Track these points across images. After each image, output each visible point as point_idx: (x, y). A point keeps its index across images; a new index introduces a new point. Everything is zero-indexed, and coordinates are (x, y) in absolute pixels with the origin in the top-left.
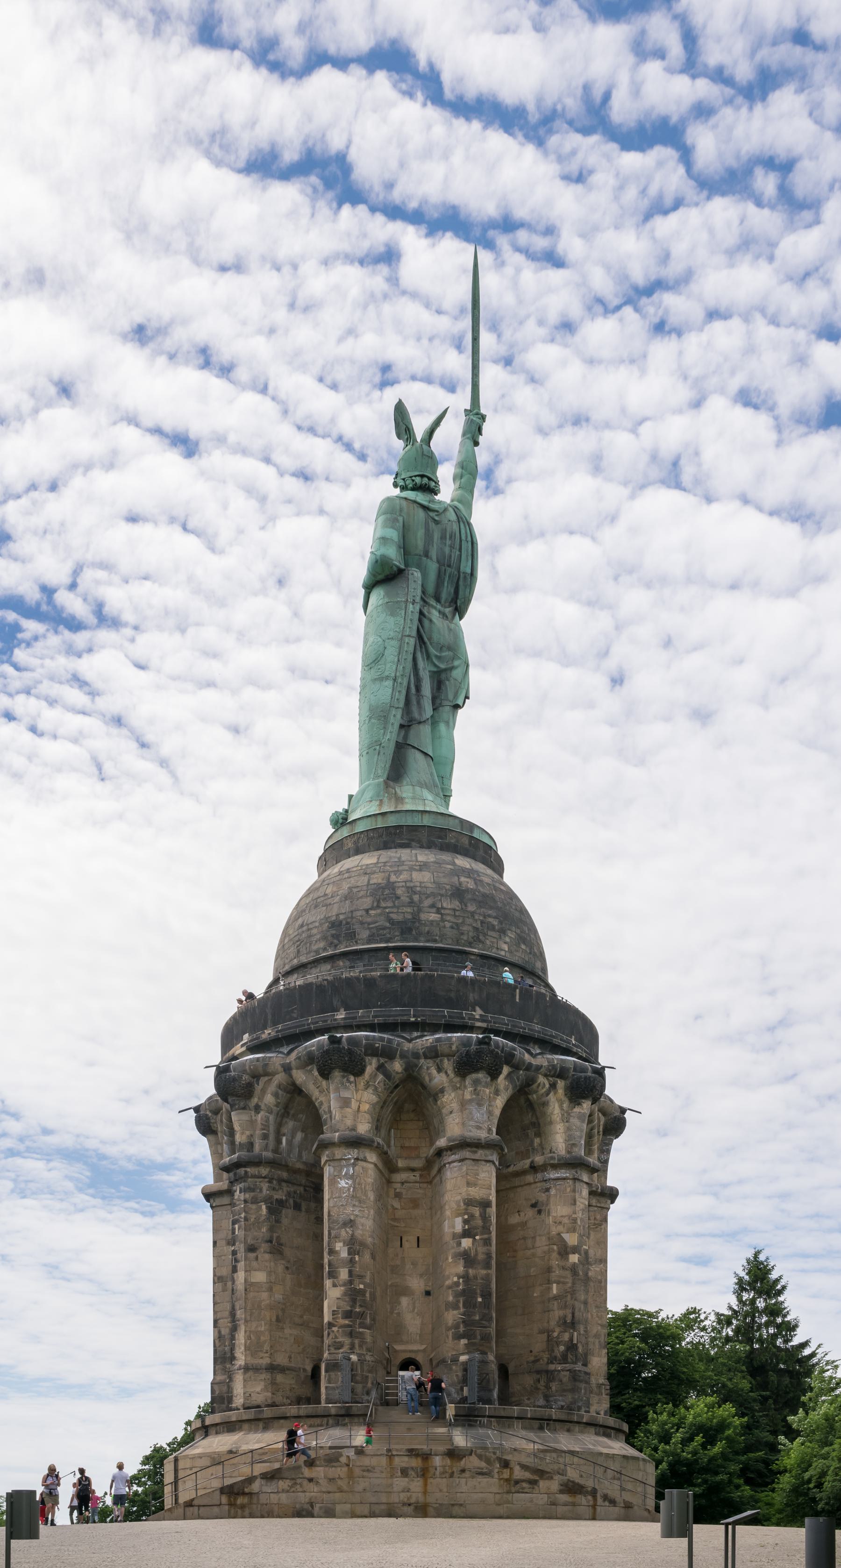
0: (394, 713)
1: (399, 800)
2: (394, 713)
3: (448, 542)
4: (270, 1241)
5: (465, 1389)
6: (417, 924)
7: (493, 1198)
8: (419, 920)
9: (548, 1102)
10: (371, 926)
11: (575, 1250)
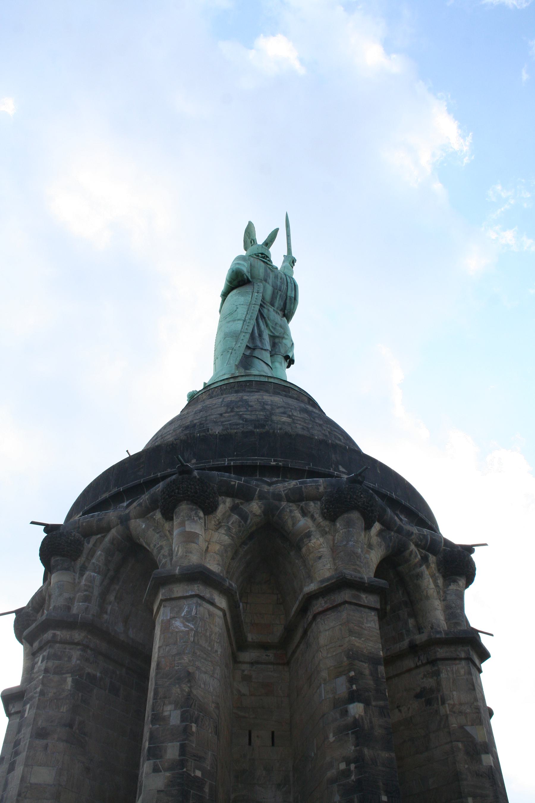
4: (70, 725)
6: (270, 423)
8: (272, 421)
9: (422, 573)
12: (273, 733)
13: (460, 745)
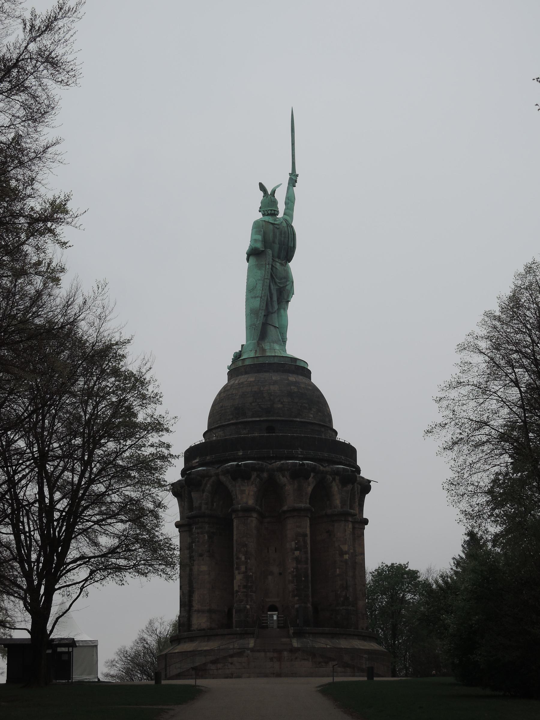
0: (261, 312)
1: (264, 350)
2: (261, 312)
3: (283, 236)
5: (298, 620)
7: (308, 532)
10: (253, 410)
11: (346, 553)
12: (276, 548)
13: (337, 552)
